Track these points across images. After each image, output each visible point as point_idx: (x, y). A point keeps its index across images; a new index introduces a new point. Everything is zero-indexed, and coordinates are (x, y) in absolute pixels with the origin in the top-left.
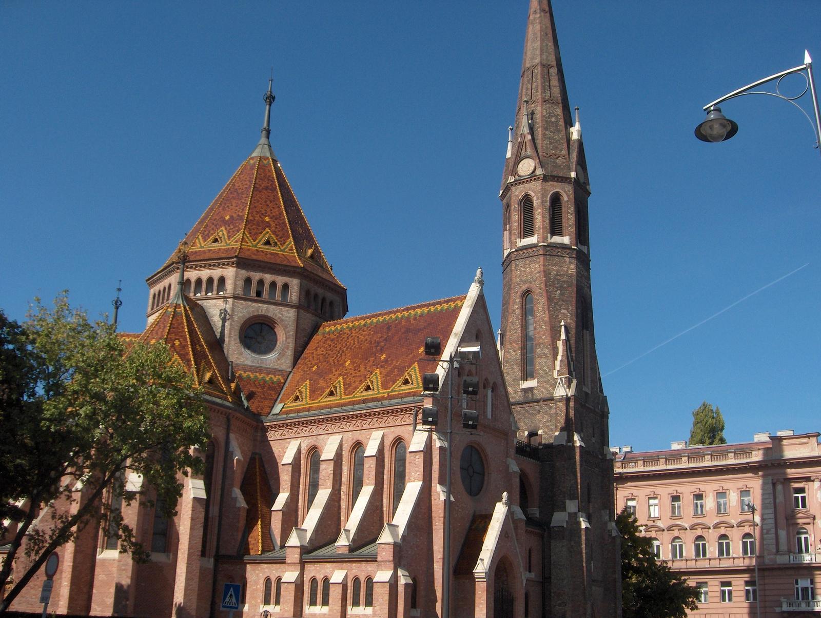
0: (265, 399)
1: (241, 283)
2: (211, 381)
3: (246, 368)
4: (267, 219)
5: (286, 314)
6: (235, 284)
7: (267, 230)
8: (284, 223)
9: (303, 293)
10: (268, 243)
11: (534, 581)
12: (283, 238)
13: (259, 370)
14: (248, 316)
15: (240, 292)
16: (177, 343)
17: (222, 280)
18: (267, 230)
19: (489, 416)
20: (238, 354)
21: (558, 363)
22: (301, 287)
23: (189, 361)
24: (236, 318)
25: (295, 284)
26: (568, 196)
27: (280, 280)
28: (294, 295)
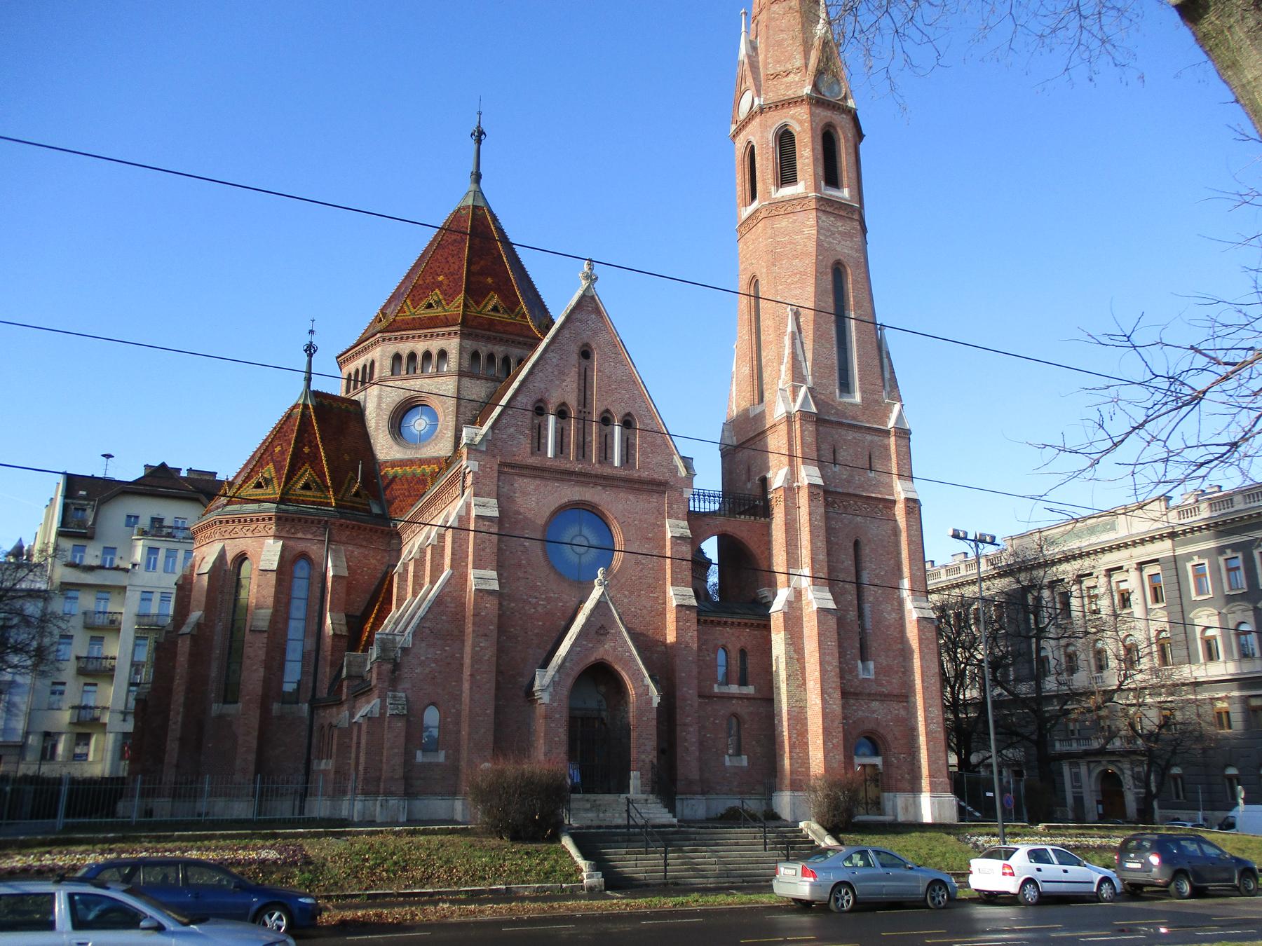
0: (409, 496)
1: (388, 363)
2: (306, 487)
3: (394, 464)
4: (441, 278)
5: (444, 387)
6: (381, 365)
7: (437, 291)
8: (461, 278)
9: (466, 356)
10: (430, 306)
11: (748, 699)
12: (449, 297)
13: (410, 462)
14: (398, 400)
15: (388, 373)
16: (278, 449)
17: (373, 363)
18: (437, 291)
19: (617, 463)
20: (385, 448)
21: (783, 368)
22: (462, 350)
23: (282, 468)
24: (384, 406)
25: (452, 345)
26: (801, 122)
27: (434, 346)
28: (453, 362)
